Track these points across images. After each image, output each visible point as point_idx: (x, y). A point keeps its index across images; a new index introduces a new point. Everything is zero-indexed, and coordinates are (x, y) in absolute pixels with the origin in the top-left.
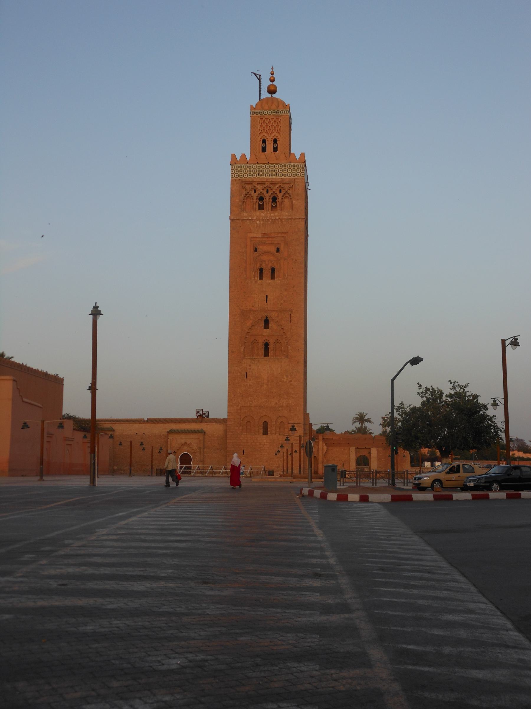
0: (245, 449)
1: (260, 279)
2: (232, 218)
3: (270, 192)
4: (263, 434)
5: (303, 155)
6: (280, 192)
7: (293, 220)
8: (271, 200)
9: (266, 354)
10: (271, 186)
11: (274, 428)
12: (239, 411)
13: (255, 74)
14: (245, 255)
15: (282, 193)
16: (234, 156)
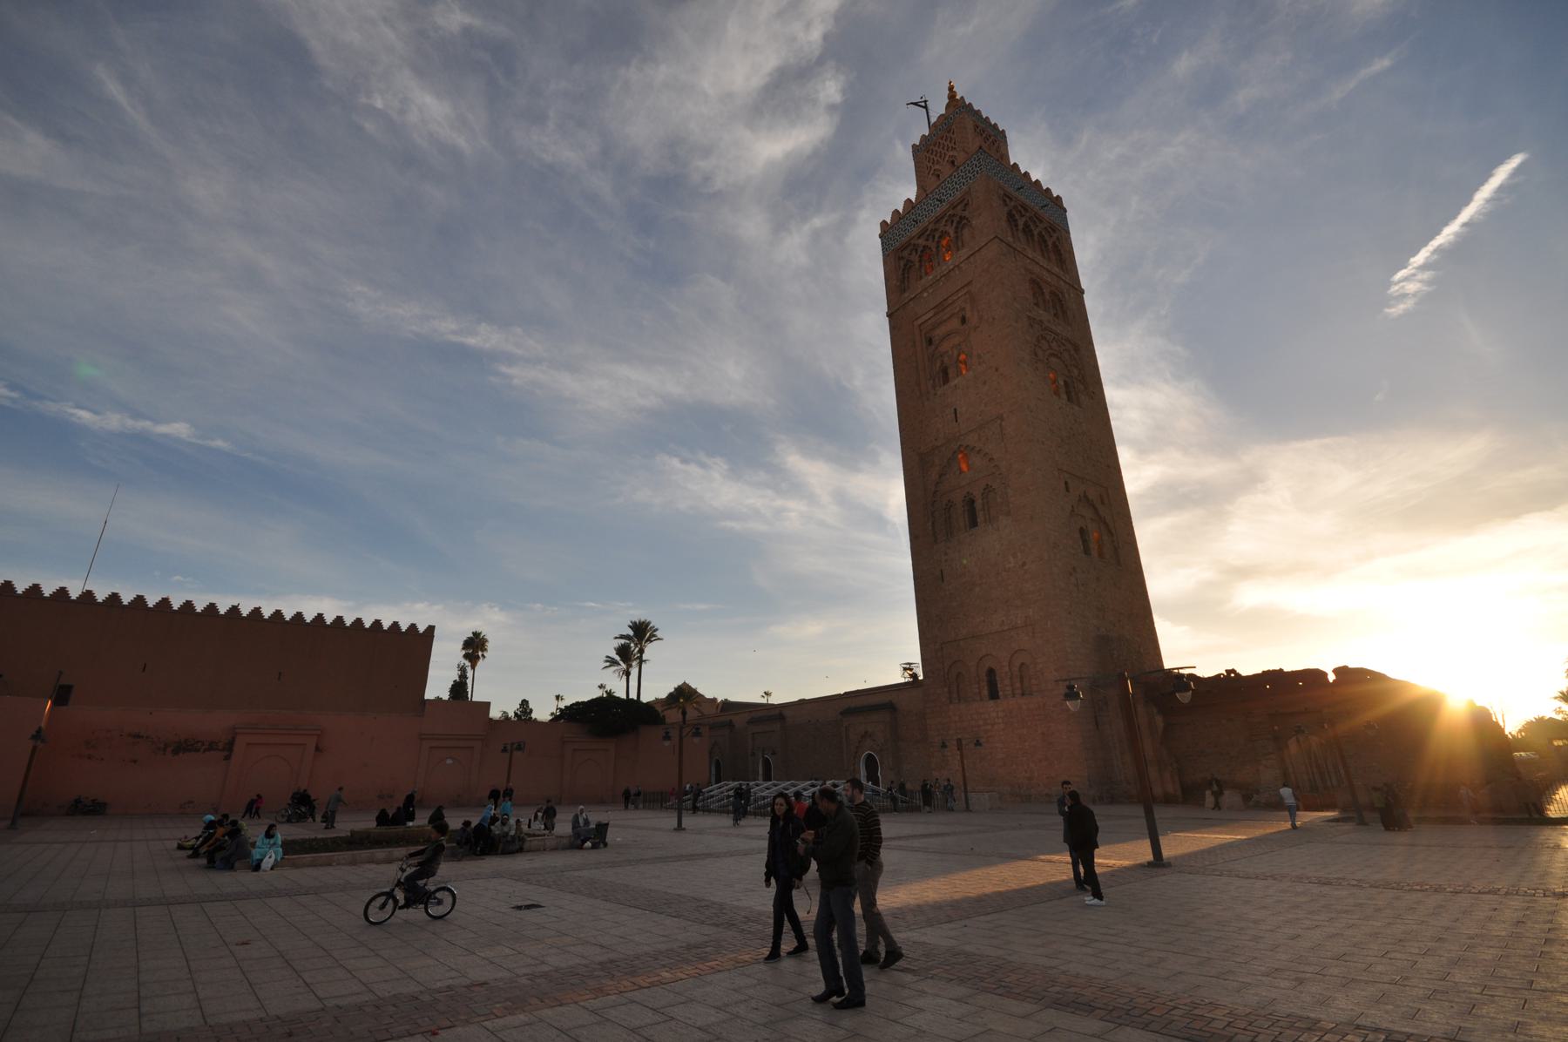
11: (1007, 682)
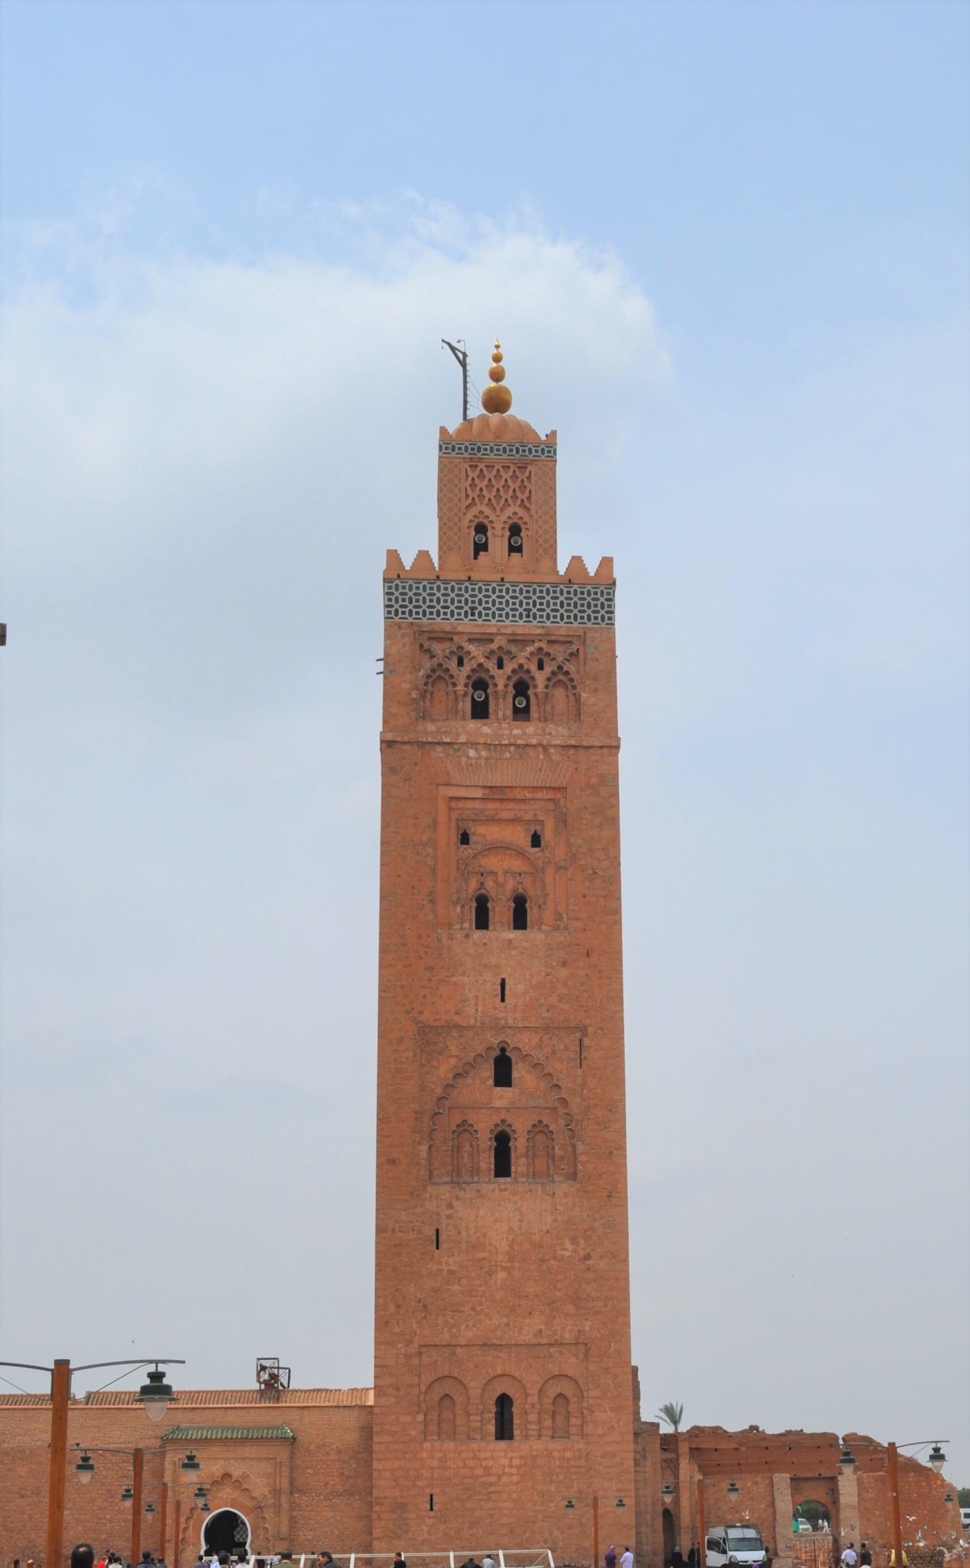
0: (436, 1491)
1: (478, 927)
2: (389, 736)
3: (509, 667)
4: (497, 1439)
5: (607, 563)
6: (541, 667)
7: (581, 751)
8: (511, 691)
9: (502, 1168)
10: (513, 649)
11: (533, 1417)
12: (415, 1361)
13: (453, 349)
14: (430, 851)
15: (548, 670)
16: (393, 556)
